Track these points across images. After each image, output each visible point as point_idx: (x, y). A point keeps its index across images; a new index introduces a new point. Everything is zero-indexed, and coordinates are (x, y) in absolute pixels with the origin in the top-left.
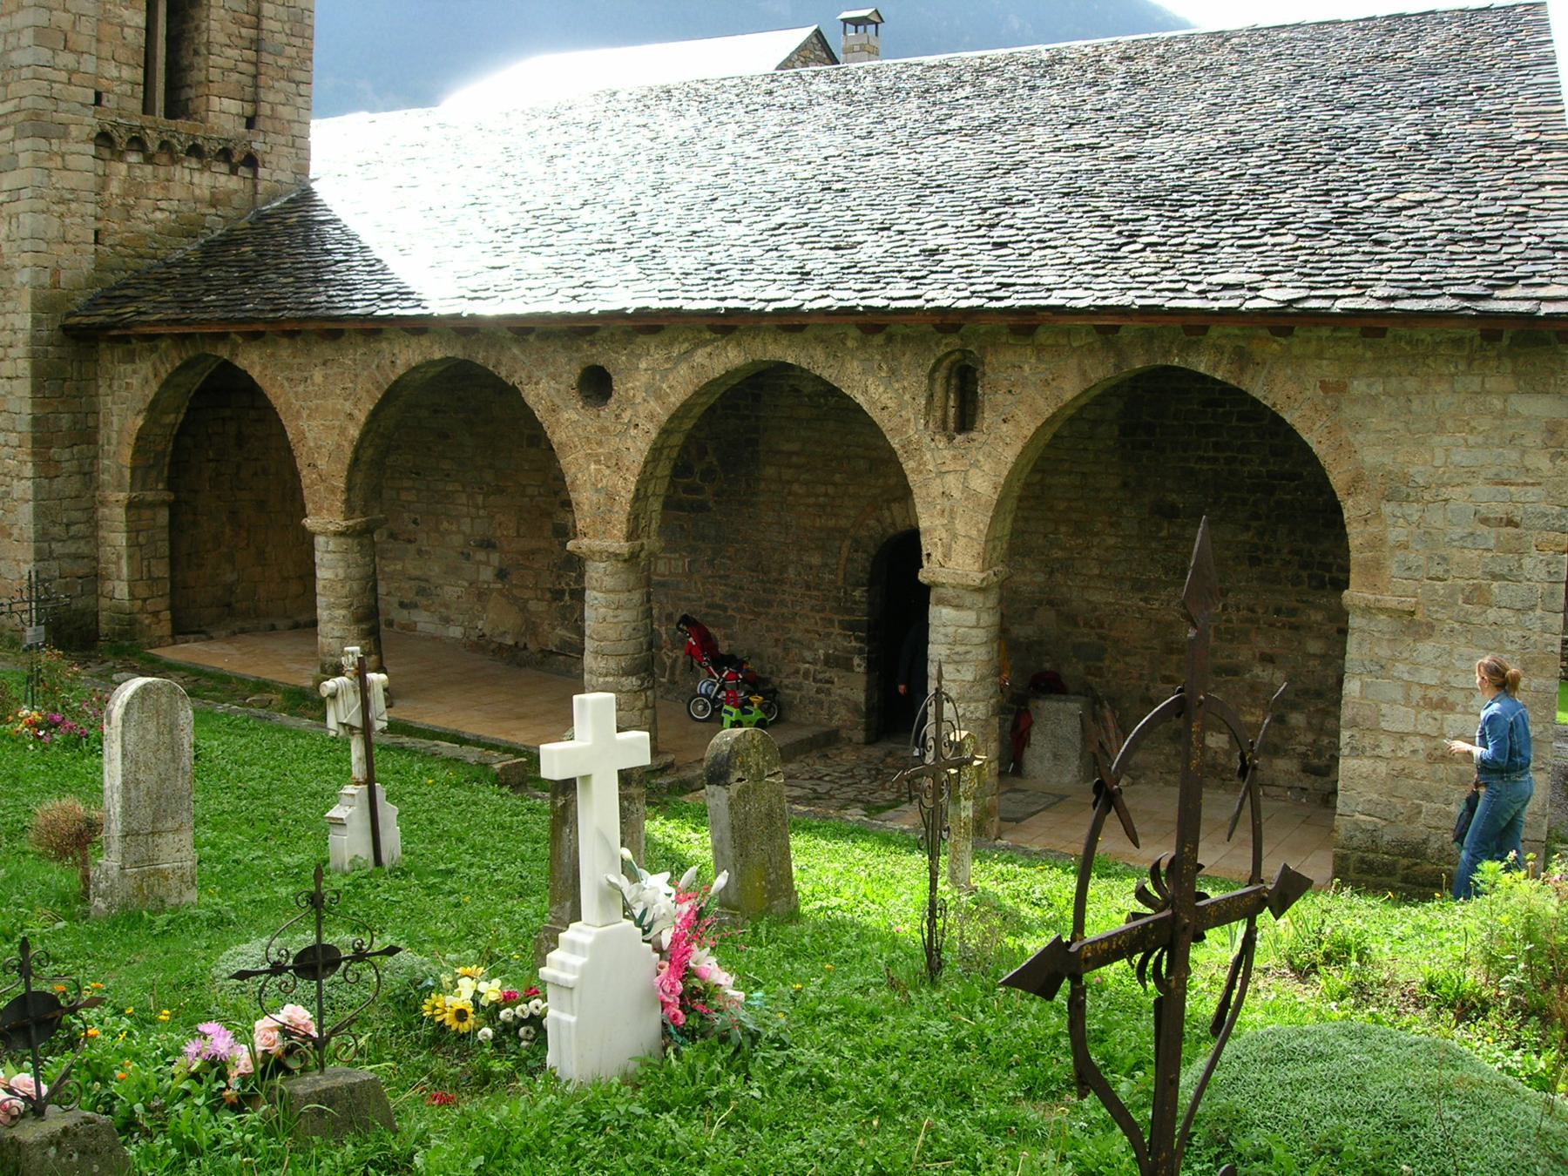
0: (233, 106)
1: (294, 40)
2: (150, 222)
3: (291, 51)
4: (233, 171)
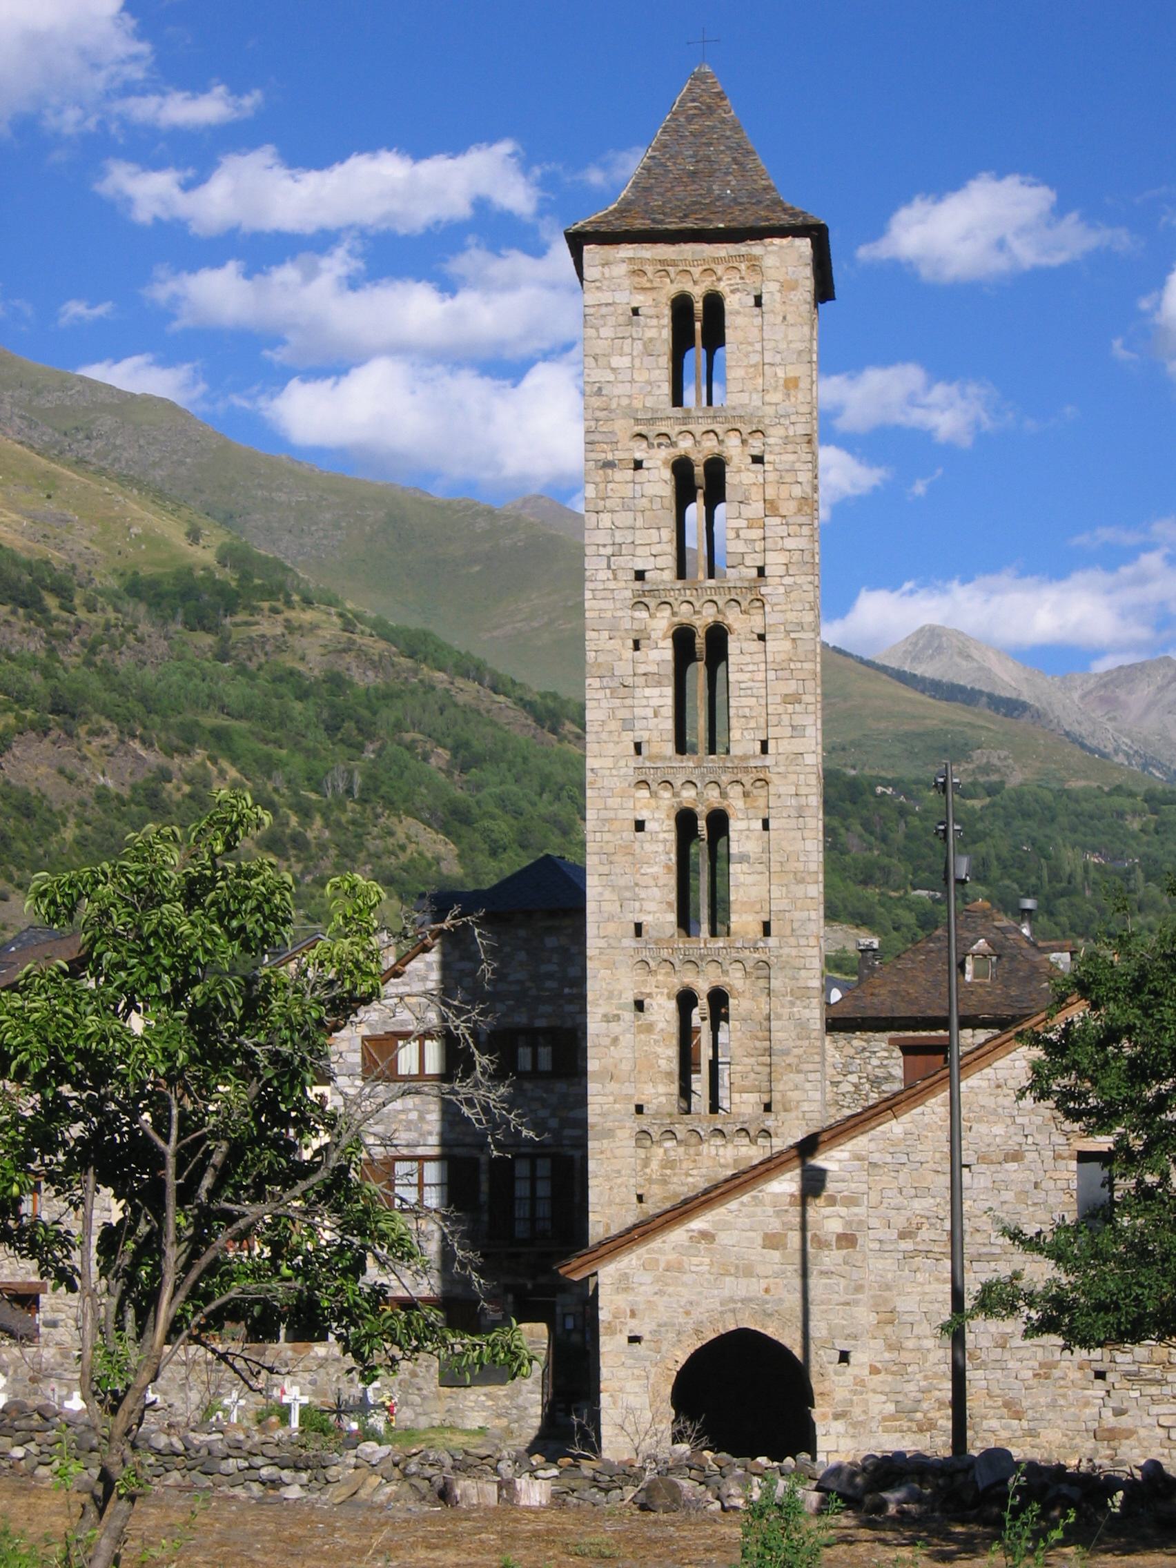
0: (753, 1098)
1: (799, 1043)
2: (683, 1184)
3: (796, 1051)
4: (753, 1141)
